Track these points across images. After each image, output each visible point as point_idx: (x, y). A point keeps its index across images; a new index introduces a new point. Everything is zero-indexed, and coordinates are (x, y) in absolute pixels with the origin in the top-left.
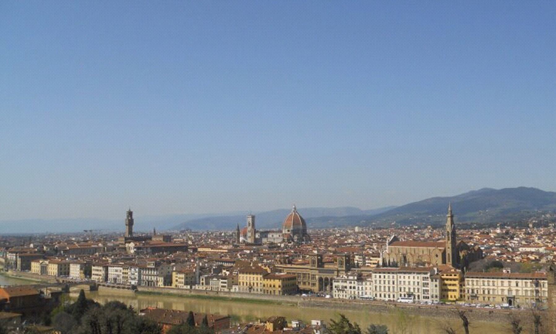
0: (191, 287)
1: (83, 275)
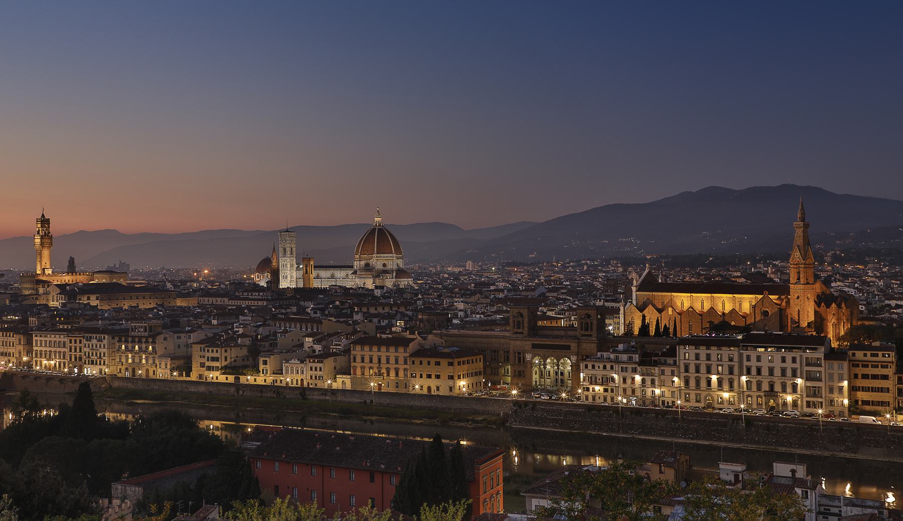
0: (237, 379)
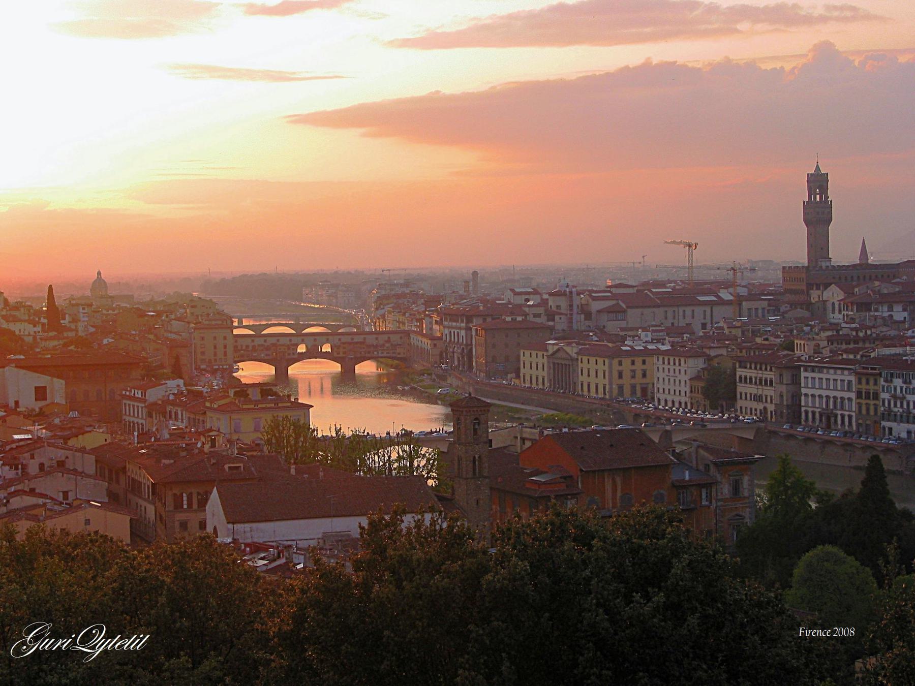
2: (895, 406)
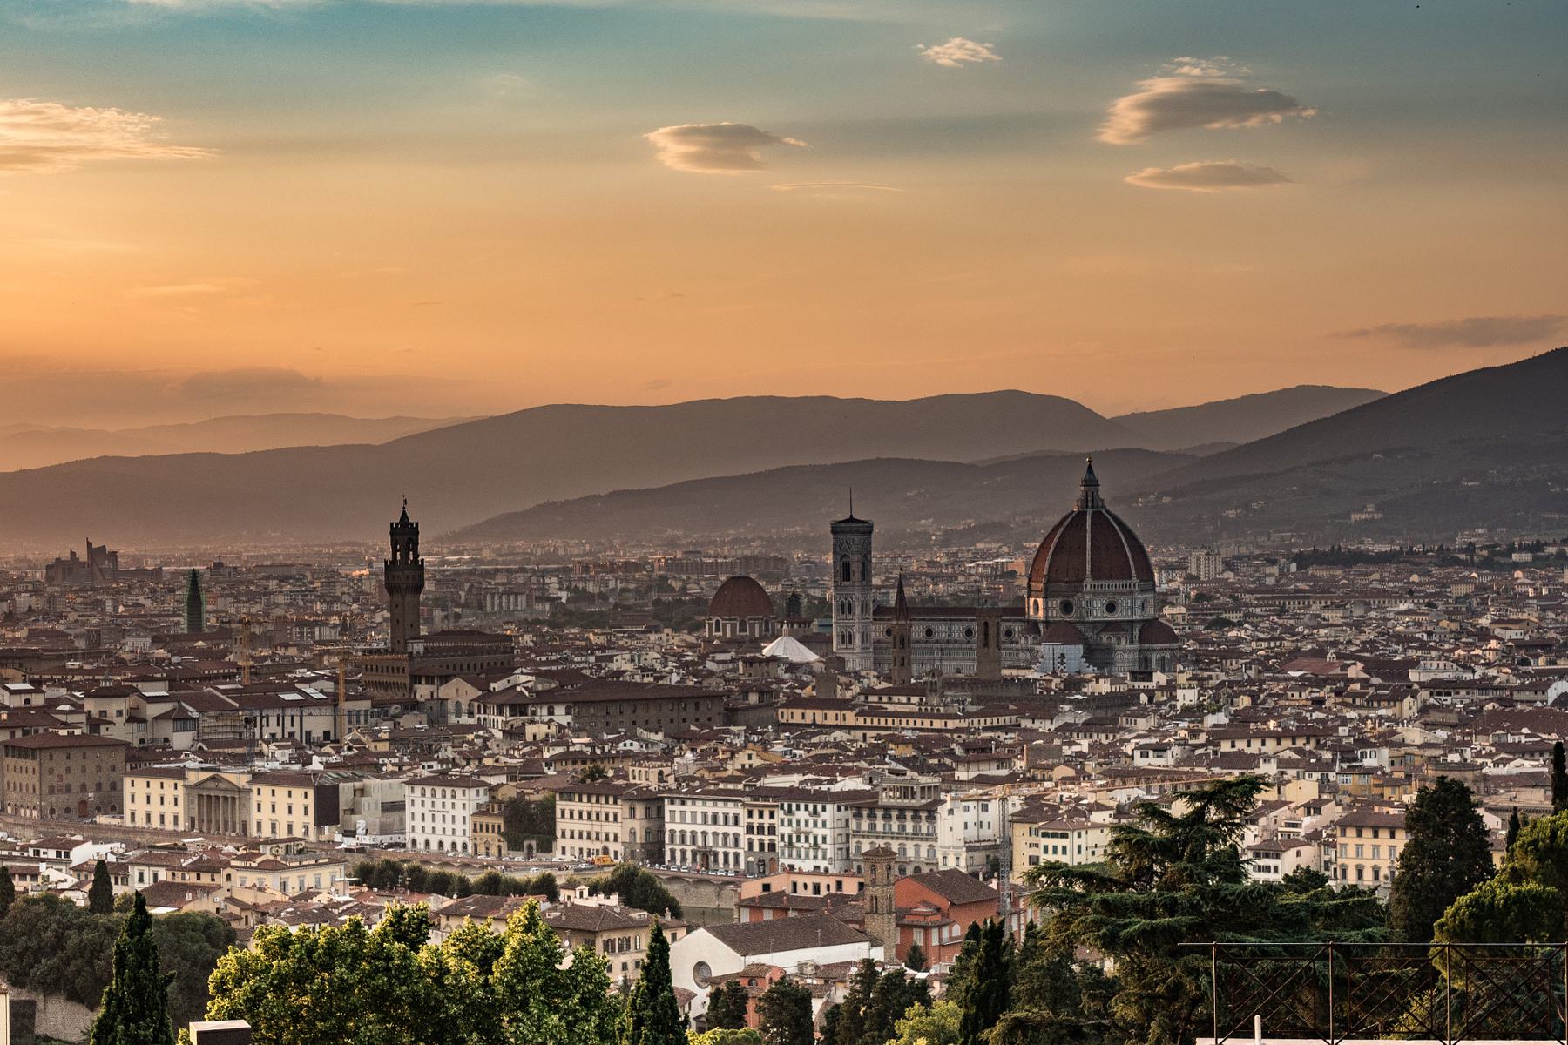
1: (494, 839)
2: (798, 840)
